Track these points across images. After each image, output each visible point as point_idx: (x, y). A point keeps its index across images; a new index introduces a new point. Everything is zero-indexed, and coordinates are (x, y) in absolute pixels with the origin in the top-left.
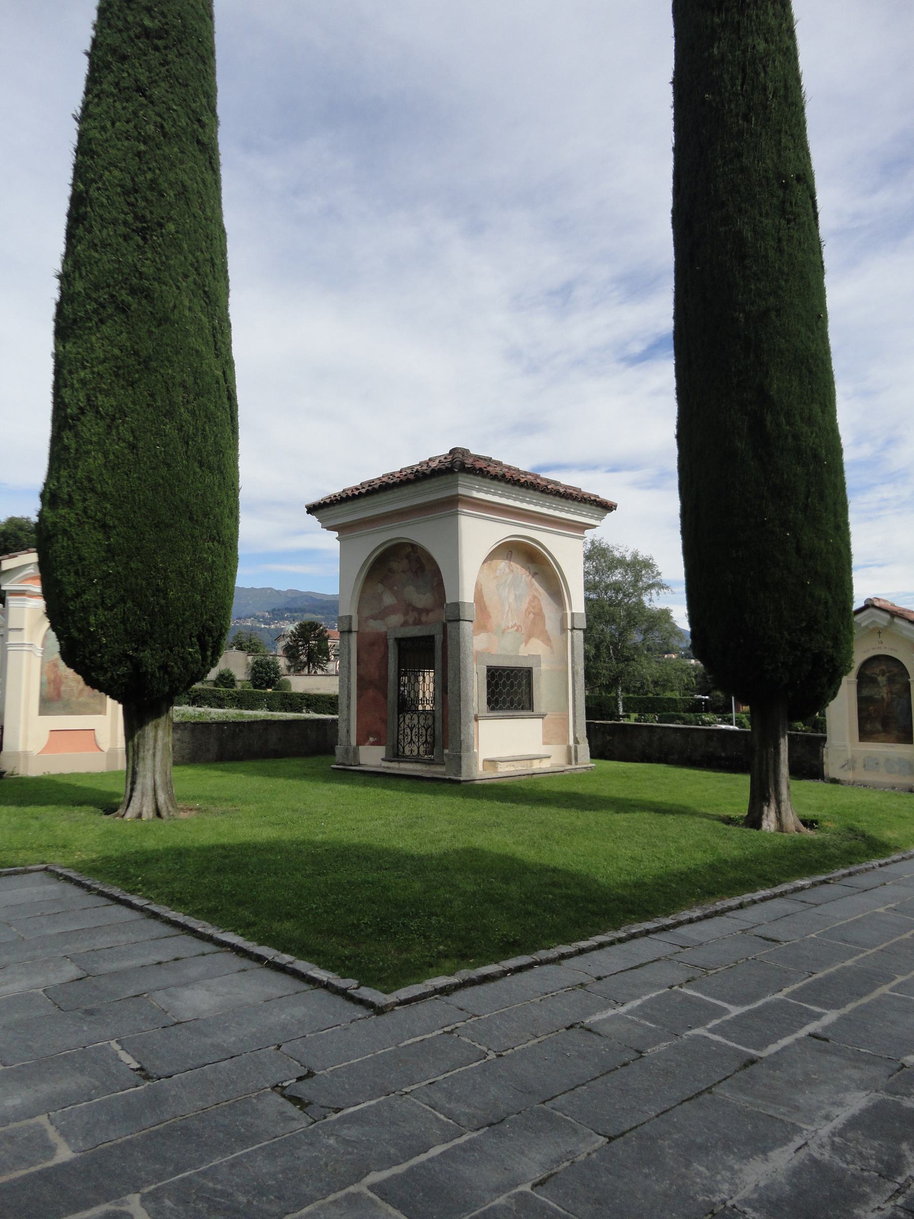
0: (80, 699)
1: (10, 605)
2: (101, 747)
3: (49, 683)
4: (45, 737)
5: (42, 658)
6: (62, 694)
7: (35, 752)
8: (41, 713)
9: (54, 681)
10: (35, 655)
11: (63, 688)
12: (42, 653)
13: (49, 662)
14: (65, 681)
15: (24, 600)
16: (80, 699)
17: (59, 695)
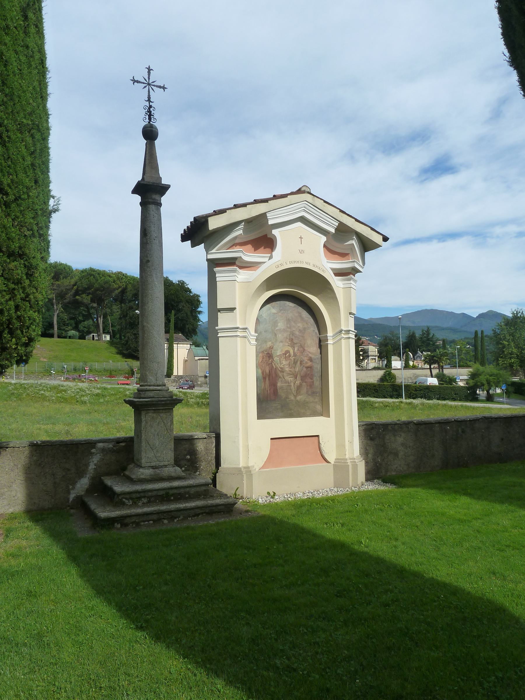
0: (299, 398)
1: (218, 279)
2: (326, 457)
3: (264, 378)
4: (266, 447)
5: (257, 346)
6: (280, 392)
7: (257, 468)
8: (260, 417)
9: (270, 375)
10: (250, 343)
11: (279, 384)
12: (256, 340)
13: (263, 352)
14: (281, 374)
15: (234, 271)
16: (299, 398)
17: (275, 392)
